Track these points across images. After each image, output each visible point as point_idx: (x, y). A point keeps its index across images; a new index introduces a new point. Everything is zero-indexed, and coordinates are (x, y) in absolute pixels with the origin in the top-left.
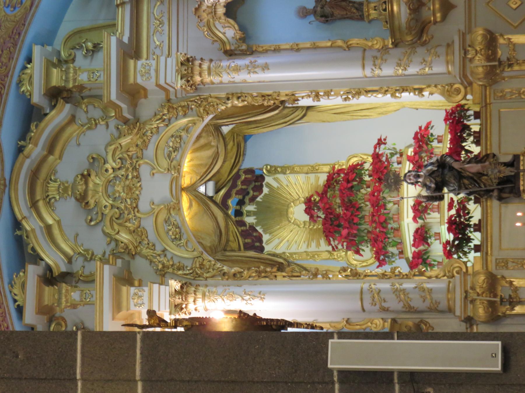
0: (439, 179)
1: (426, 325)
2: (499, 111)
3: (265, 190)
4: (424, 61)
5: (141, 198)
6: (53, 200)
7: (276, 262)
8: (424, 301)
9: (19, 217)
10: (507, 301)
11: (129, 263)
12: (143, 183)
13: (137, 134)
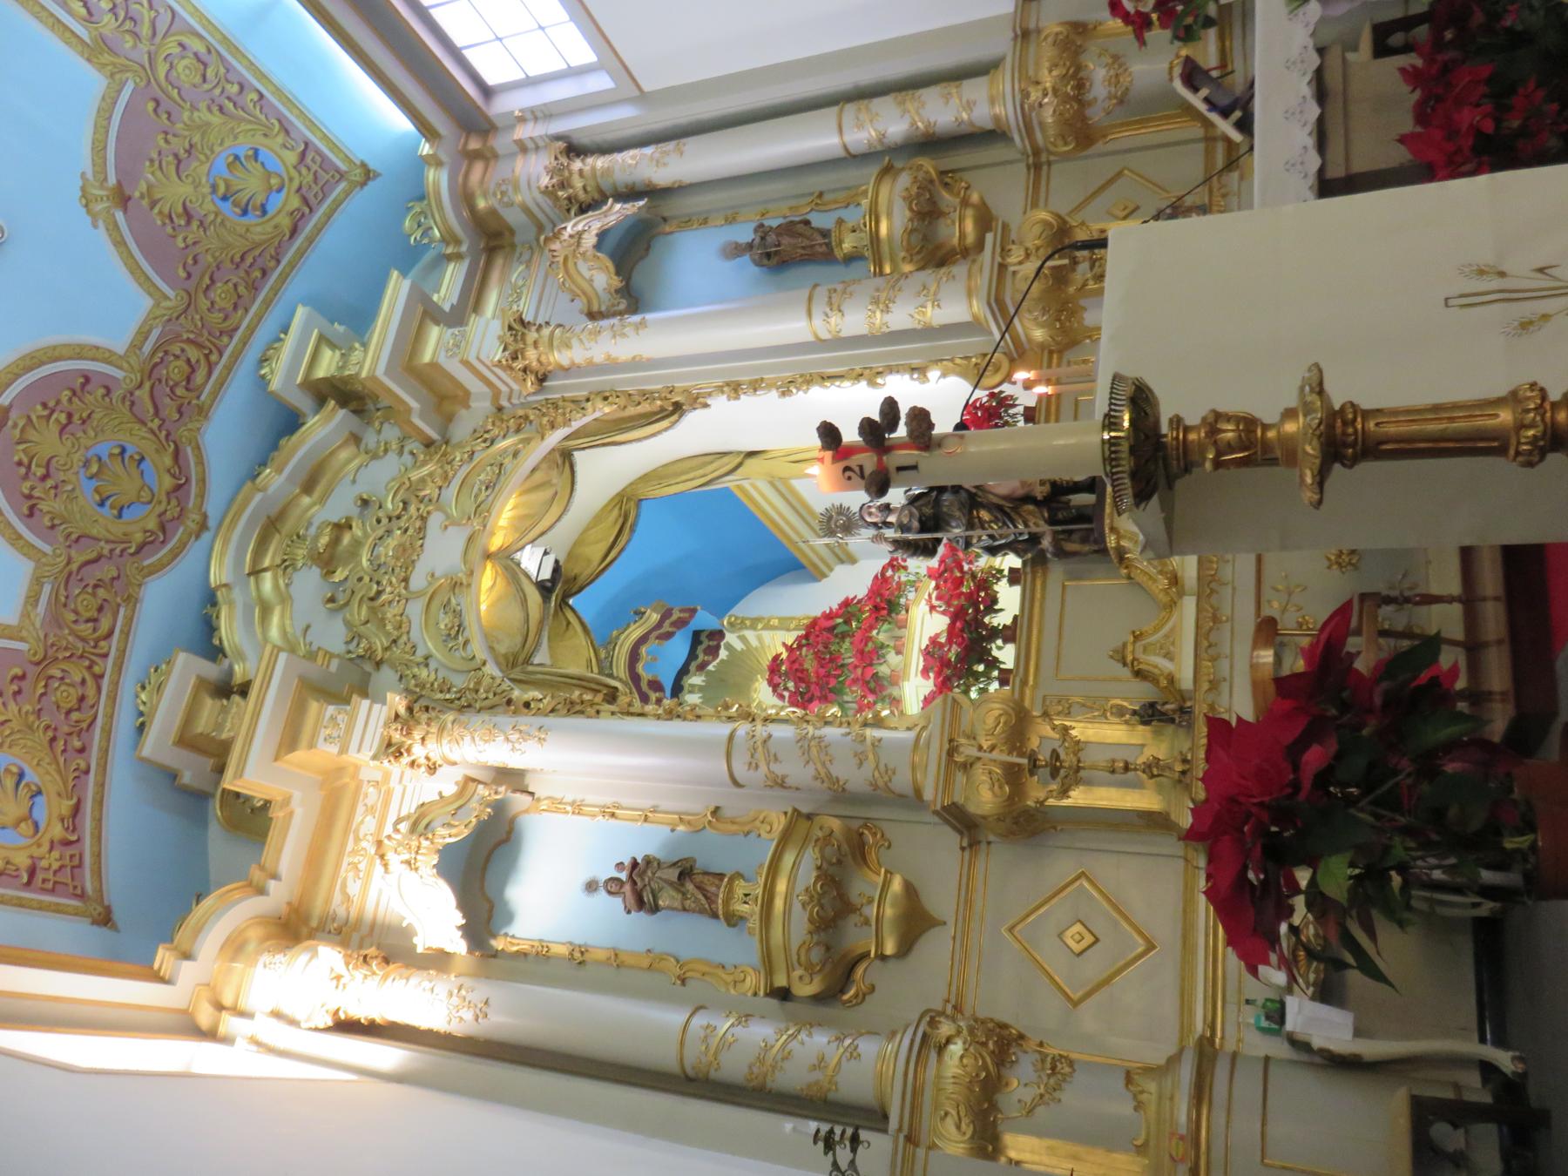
0: (928, 511)
1: (874, 835)
2: (1077, 401)
3: (723, 654)
4: (924, 288)
5: (418, 565)
7: (607, 686)
8: (861, 763)
10: (1046, 766)
11: (370, 674)
12: (428, 542)
13: (438, 461)
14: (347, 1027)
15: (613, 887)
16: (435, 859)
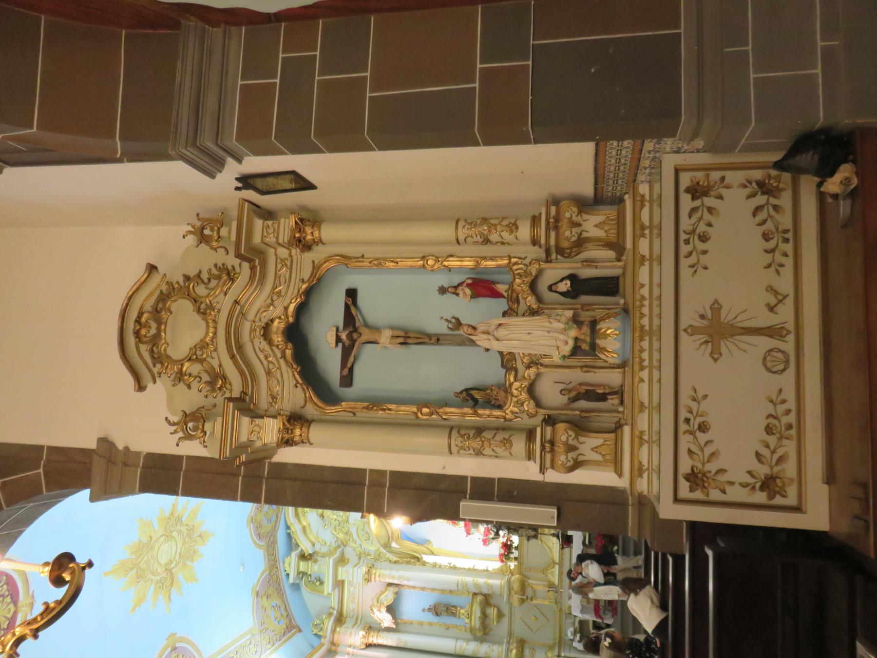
6: (306, 513)
9: (289, 524)
14: (369, 646)
15: (429, 610)
16: (386, 609)
